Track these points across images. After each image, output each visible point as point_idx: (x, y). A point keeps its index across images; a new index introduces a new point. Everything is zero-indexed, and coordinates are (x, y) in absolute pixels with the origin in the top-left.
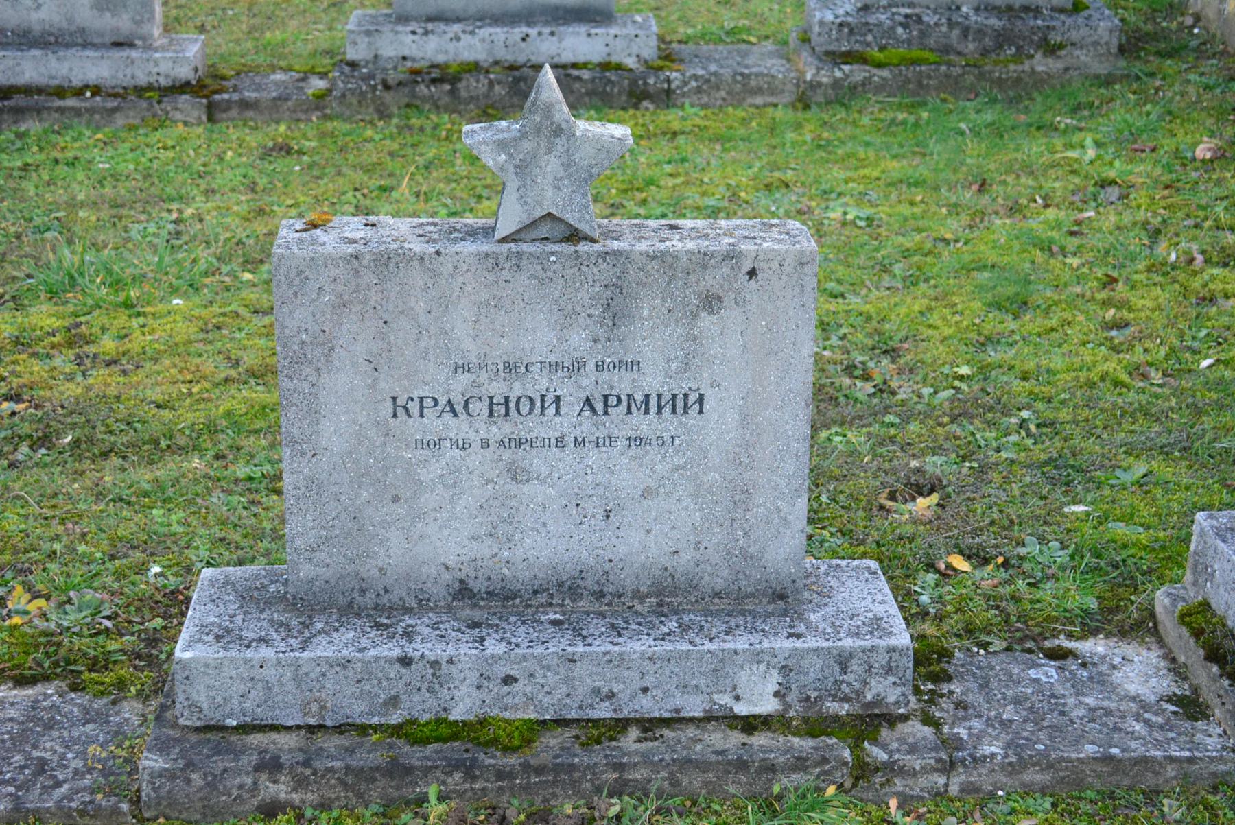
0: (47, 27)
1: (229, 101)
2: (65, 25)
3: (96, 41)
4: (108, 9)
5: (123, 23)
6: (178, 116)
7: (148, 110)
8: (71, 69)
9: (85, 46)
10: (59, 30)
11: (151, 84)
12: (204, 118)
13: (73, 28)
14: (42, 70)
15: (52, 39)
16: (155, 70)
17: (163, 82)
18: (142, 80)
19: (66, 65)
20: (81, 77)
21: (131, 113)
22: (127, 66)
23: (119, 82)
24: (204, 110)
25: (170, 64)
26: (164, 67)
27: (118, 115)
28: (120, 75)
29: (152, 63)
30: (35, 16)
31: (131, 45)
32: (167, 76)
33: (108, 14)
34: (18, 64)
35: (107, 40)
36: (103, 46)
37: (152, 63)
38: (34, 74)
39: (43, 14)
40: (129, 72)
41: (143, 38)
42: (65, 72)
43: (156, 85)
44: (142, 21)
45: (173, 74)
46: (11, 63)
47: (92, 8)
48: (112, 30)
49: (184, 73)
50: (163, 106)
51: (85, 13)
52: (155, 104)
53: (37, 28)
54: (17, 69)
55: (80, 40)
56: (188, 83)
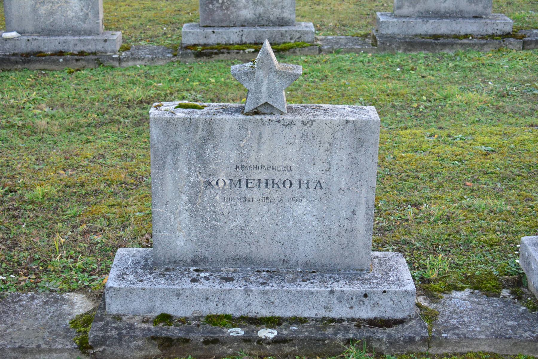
0: (447, 10)
1: (531, 41)
2: (454, 9)
3: (466, 16)
4: (474, 2)
5: (479, 8)
6: (511, 47)
7: (499, 44)
8: (461, 27)
9: (463, 17)
10: (452, 11)
11: (493, 34)
12: (521, 48)
13: (458, 10)
14: (449, 28)
15: (448, 15)
16: (496, 28)
17: (499, 33)
18: (490, 32)
19: (459, 25)
20: (465, 31)
21: (491, 46)
22: (485, 26)
23: (480, 33)
24: (522, 44)
25: (503, 25)
26: (500, 27)
27: (485, 46)
28: (481, 30)
29: (495, 25)
30: (443, 5)
31: (481, 17)
32: (500, 30)
33: (473, 4)
34: (440, 25)
35: (471, 15)
36: (469, 18)
37: (495, 25)
38: (445, 30)
39: (446, 5)
40: (485, 28)
41: (486, 15)
42: (458, 28)
43: (495, 34)
44: (487, 8)
45: (503, 29)
46: (436, 25)
47: (467, 2)
48: (474, 11)
49: (508, 29)
50: (505, 43)
51: (464, 5)
52: (502, 42)
53: (443, 10)
54: (439, 27)
55: (460, 16)
56: (509, 33)
